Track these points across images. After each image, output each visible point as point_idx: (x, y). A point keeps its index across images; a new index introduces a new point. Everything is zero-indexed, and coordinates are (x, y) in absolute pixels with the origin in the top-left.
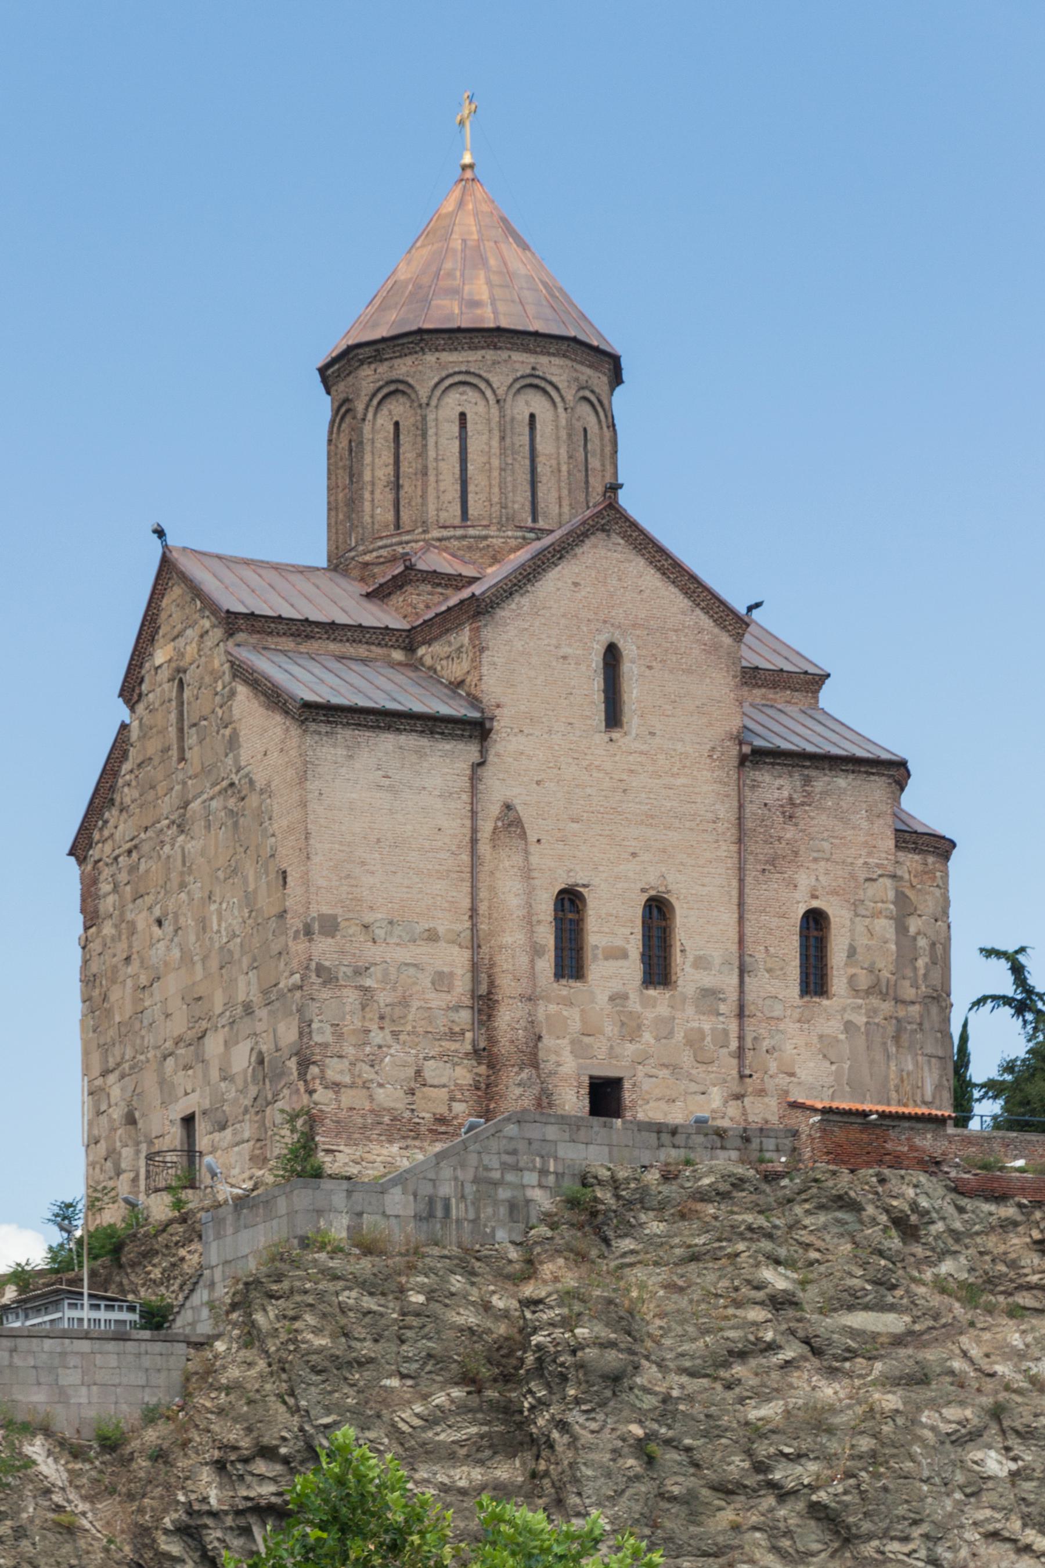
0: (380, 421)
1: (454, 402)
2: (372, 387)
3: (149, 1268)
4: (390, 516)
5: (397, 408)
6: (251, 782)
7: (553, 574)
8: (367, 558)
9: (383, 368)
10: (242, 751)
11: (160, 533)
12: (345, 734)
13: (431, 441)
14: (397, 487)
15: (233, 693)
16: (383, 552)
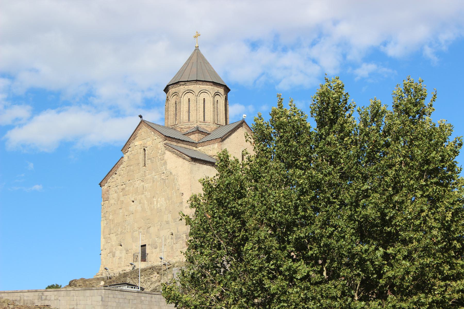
0: (185, 98)
1: (203, 96)
2: (183, 91)
4: (187, 118)
5: (189, 95)
6: (171, 173)
7: (233, 135)
8: (182, 127)
9: (186, 87)
10: (168, 166)
11: (141, 117)
12: (198, 165)
13: (198, 103)
14: (189, 112)
15: (165, 153)
16: (187, 126)
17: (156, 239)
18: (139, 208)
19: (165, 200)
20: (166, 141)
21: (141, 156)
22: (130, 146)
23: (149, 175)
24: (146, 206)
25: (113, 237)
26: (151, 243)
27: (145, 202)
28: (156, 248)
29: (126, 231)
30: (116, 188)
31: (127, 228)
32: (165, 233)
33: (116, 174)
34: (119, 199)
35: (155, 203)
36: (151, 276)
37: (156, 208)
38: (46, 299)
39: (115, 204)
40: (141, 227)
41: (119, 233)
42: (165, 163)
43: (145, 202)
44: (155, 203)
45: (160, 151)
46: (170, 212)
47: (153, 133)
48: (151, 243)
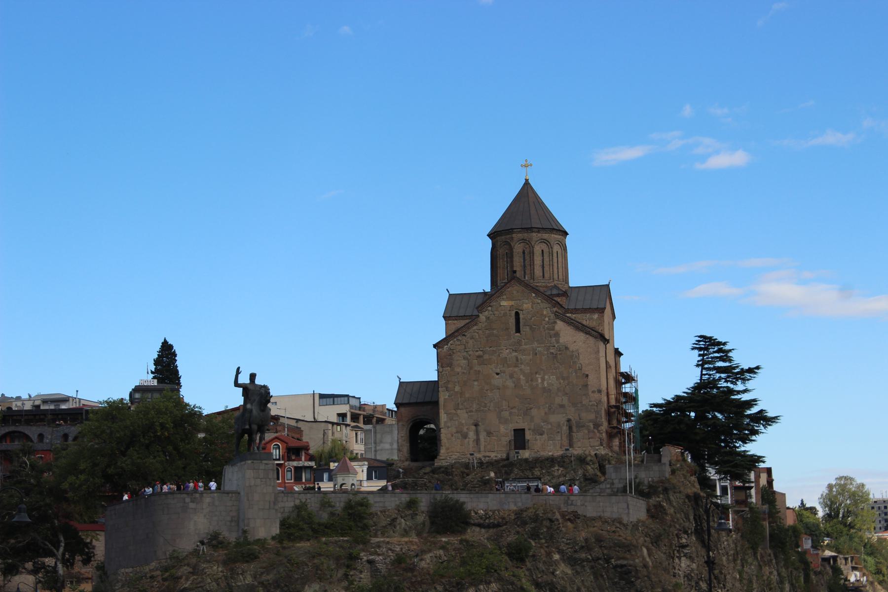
6: (567, 348)
15: (555, 322)
18: (510, 383)
19: (557, 379)
20: (555, 309)
21: (512, 321)
24: (523, 382)
25: (463, 415)
27: (521, 377)
28: (541, 434)
32: (559, 418)
34: (471, 368)
35: (540, 381)
37: (540, 386)
38: (572, 504)
42: (557, 335)
43: (521, 377)
44: (540, 381)
45: (547, 319)
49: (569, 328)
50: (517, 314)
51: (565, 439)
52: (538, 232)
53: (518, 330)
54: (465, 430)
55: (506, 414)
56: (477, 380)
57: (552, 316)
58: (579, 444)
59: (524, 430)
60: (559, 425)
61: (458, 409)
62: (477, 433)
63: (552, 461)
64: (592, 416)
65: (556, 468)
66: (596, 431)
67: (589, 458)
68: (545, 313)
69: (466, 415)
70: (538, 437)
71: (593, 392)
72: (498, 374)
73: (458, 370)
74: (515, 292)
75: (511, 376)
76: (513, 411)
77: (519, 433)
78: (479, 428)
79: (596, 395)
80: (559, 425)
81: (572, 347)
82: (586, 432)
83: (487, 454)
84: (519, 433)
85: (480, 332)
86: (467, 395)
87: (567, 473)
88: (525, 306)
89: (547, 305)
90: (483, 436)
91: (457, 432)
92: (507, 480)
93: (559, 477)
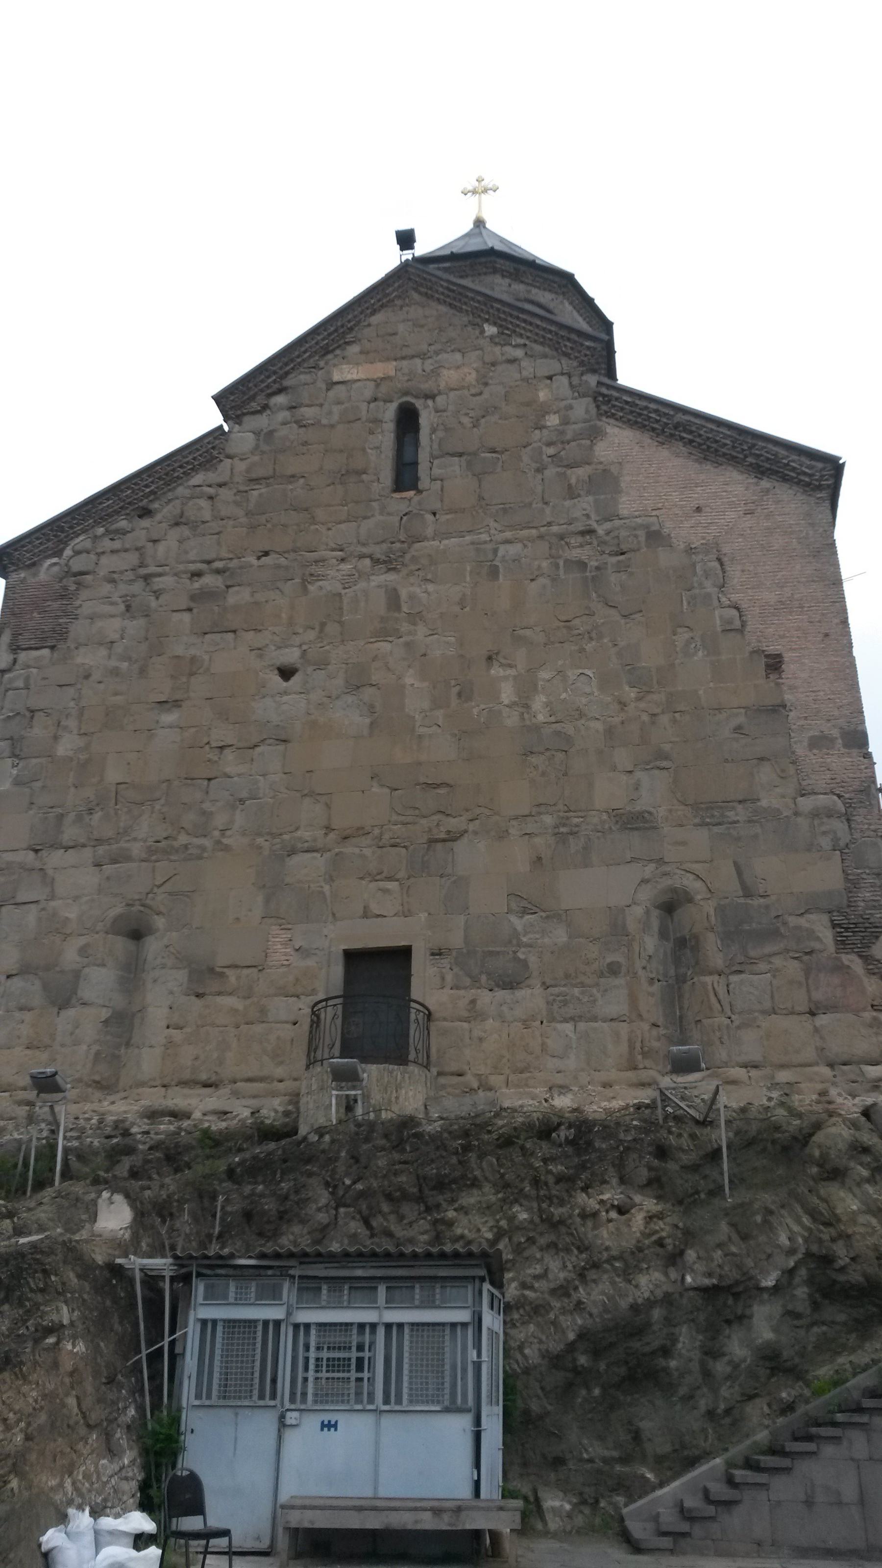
3: (451, 1214)
6: (655, 537)
15: (594, 434)
17: (518, 923)
22: (286, 383)
23: (440, 535)
24: (416, 703)
26: (456, 940)
28: (510, 984)
29: (207, 842)
30: (137, 587)
31: (220, 820)
33: (146, 513)
35: (507, 694)
36: (581, 1198)
39: (115, 672)
40: (361, 831)
41: (136, 849)
42: (605, 481)
43: (408, 680)
44: (507, 694)
45: (553, 420)
46: (662, 755)
47: (491, 330)
48: (456, 940)
49: (664, 453)
50: (407, 420)
51: (650, 1002)
52: (516, 276)
53: (405, 476)
54: (70, 956)
55: (306, 868)
56: (177, 704)
57: (582, 408)
58: (750, 1045)
59: (404, 954)
60: (617, 930)
61: (56, 845)
62: (132, 974)
63: (578, 1146)
64: (826, 876)
65: (611, 1194)
66: (856, 965)
67: (837, 1134)
68: (543, 395)
69: (89, 879)
70: (485, 998)
71: (818, 742)
72: (286, 673)
73: (90, 658)
74: (401, 328)
75: (357, 682)
76: (349, 849)
77: (377, 973)
78: (152, 946)
79: (839, 760)
80: (617, 930)
81: (684, 532)
82: (793, 968)
83: (178, 1099)
84: (377, 973)
85: (226, 494)
86: (113, 775)
87: (689, 1236)
88: (449, 376)
89: (553, 365)
90: (163, 995)
91: (25, 970)
92: (216, 1268)
93: (630, 1263)
